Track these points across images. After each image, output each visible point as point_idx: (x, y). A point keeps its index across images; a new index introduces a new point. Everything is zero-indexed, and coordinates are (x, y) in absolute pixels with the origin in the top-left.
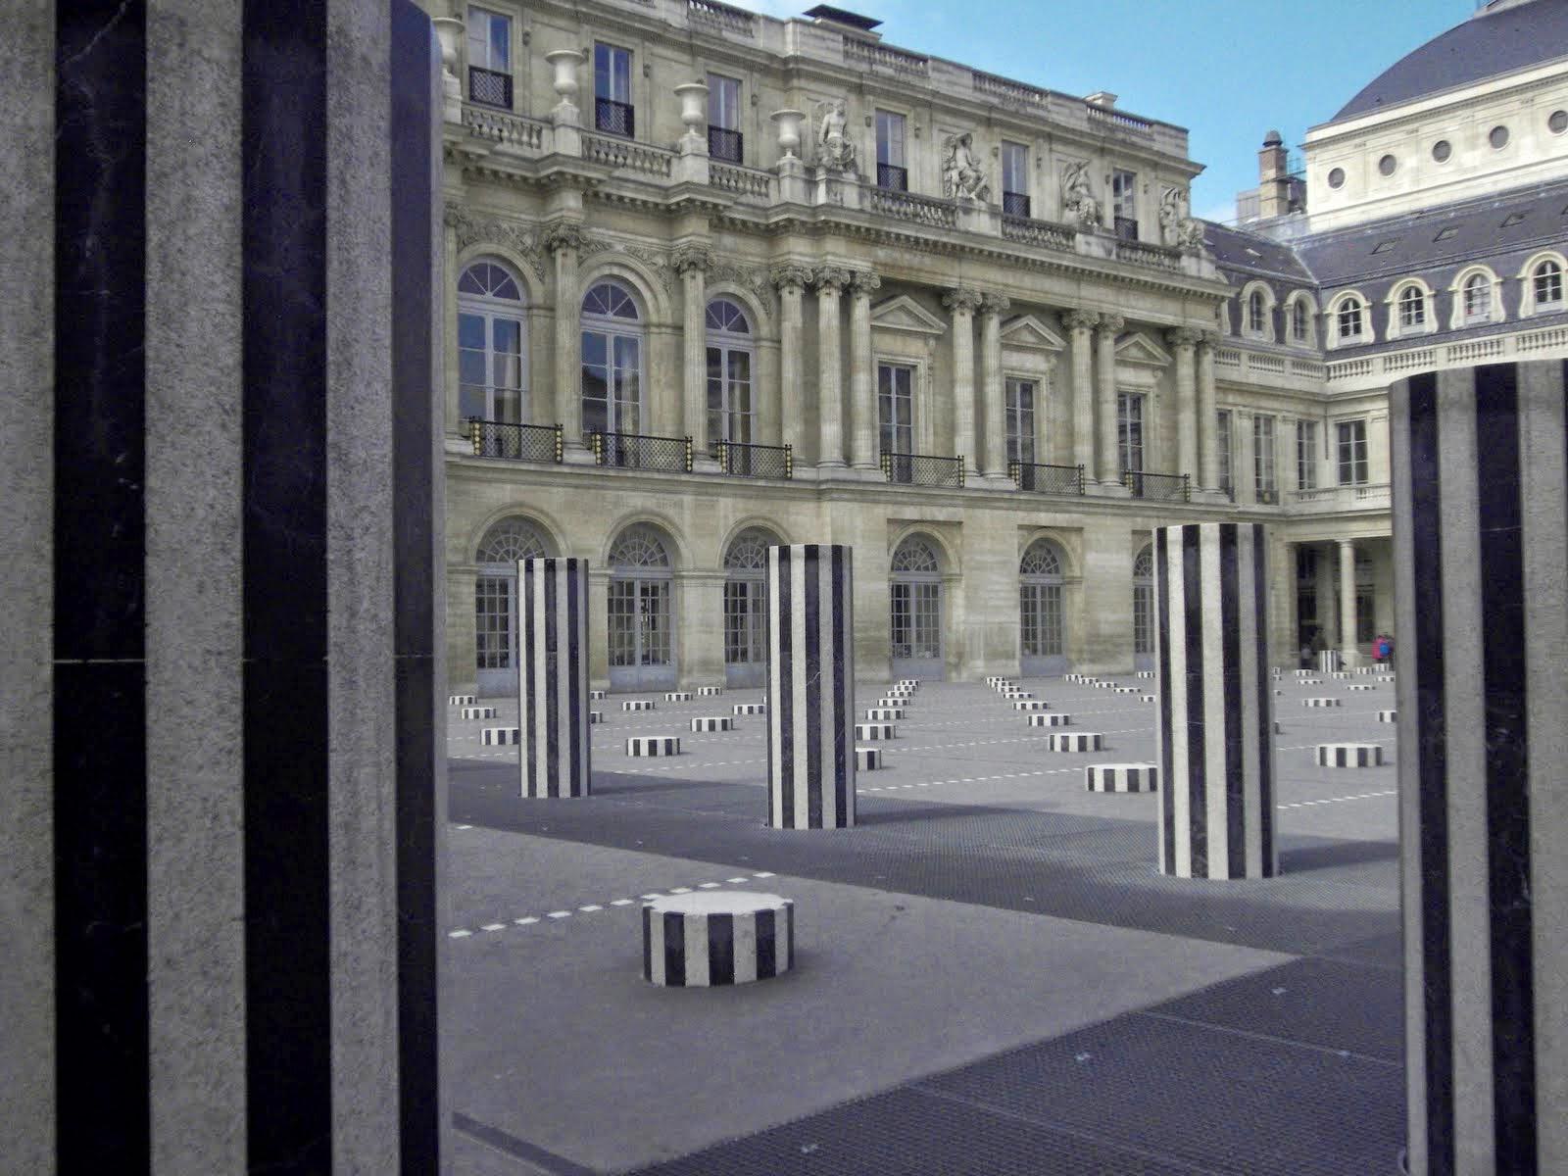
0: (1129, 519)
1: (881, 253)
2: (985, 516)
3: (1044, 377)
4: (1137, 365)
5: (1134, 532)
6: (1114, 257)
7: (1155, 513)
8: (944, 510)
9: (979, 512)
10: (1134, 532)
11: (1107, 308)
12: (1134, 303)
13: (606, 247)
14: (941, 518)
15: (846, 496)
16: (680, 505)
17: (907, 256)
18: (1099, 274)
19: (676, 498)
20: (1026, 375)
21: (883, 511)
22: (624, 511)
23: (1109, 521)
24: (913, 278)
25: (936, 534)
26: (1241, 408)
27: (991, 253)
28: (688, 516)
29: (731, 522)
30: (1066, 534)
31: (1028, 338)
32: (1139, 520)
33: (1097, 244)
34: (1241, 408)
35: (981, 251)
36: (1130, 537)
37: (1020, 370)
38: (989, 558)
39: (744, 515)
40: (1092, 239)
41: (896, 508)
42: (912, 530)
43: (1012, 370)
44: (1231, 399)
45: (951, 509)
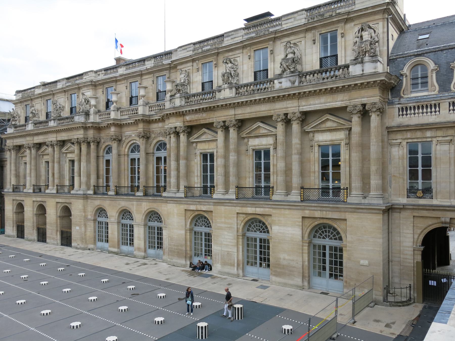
0: (301, 211)
1: (188, 118)
2: (222, 208)
3: (271, 146)
4: (330, 130)
5: (303, 217)
6: (297, 84)
7: (319, 209)
8: (205, 207)
9: (219, 207)
10: (303, 217)
11: (290, 111)
12: (312, 103)
13: (130, 136)
14: (204, 210)
15: (171, 202)
16: (133, 205)
17: (197, 116)
18: (279, 97)
19: (131, 203)
20: (264, 147)
21: (183, 207)
22: (120, 206)
23: (287, 212)
24: (198, 123)
25: (206, 215)
26: (440, 139)
27: (222, 105)
28: (135, 208)
29: (146, 209)
30: (266, 217)
31: (263, 131)
32: (307, 212)
33: (286, 81)
34: (440, 139)
35: (218, 106)
36: (301, 220)
37: (259, 146)
38: (223, 225)
39: (149, 207)
40: (283, 80)
41: (188, 206)
42: (196, 213)
43: (255, 146)
44: (429, 134)
45: (208, 206)
